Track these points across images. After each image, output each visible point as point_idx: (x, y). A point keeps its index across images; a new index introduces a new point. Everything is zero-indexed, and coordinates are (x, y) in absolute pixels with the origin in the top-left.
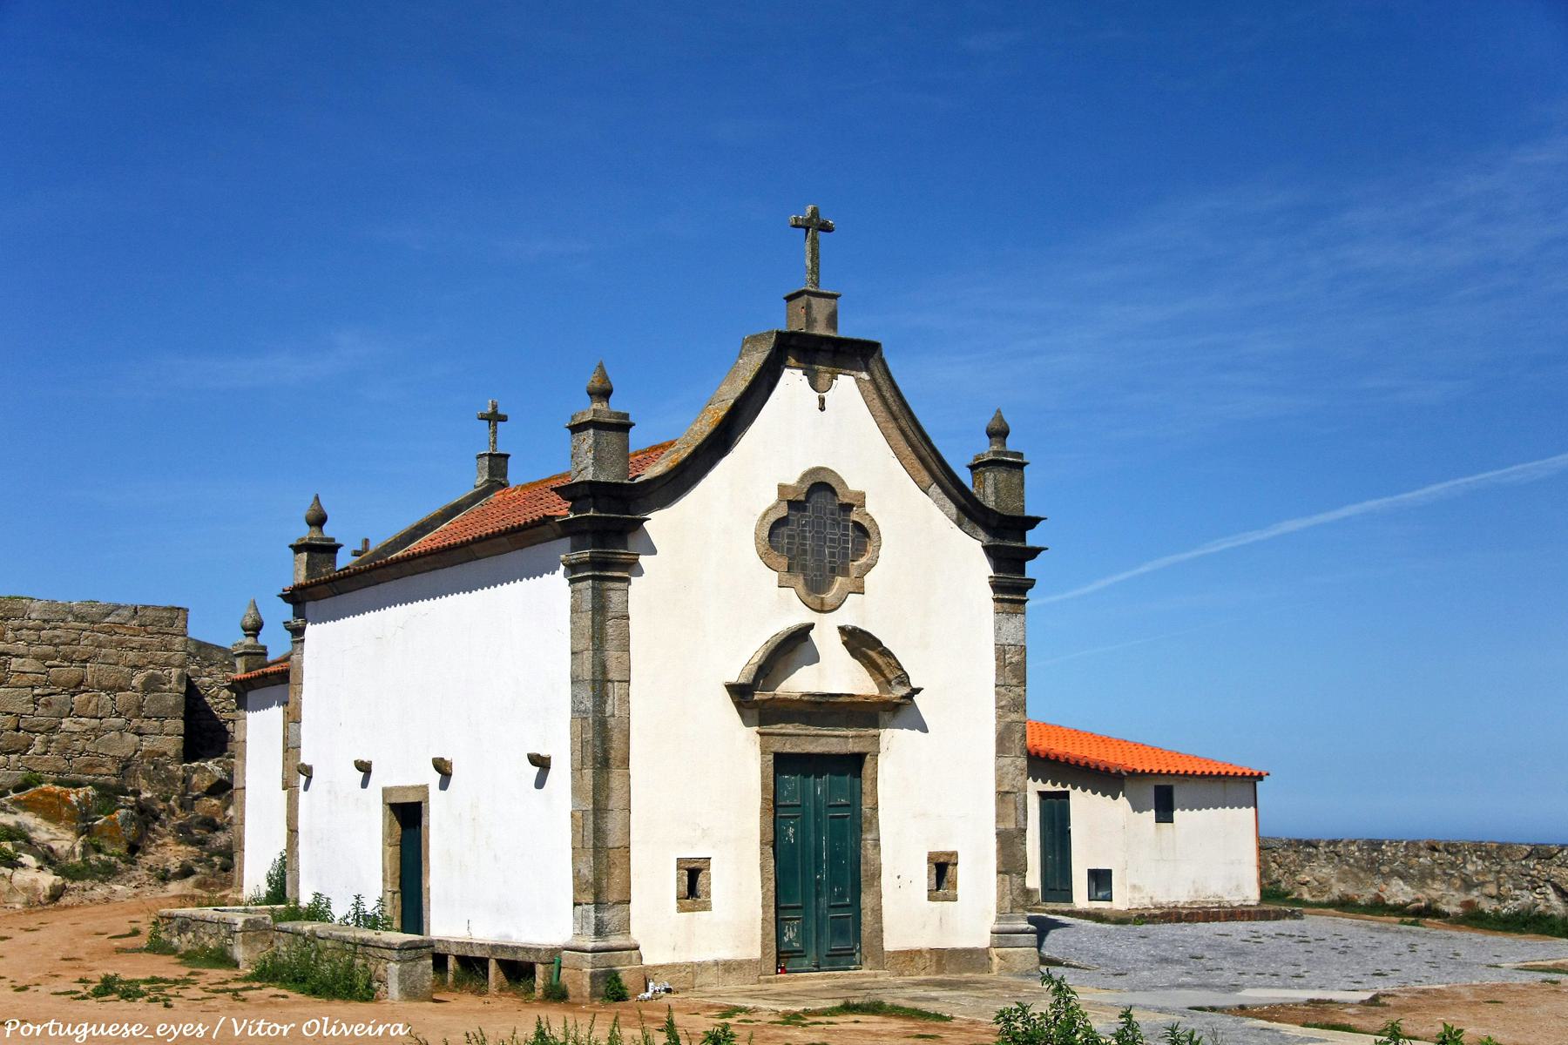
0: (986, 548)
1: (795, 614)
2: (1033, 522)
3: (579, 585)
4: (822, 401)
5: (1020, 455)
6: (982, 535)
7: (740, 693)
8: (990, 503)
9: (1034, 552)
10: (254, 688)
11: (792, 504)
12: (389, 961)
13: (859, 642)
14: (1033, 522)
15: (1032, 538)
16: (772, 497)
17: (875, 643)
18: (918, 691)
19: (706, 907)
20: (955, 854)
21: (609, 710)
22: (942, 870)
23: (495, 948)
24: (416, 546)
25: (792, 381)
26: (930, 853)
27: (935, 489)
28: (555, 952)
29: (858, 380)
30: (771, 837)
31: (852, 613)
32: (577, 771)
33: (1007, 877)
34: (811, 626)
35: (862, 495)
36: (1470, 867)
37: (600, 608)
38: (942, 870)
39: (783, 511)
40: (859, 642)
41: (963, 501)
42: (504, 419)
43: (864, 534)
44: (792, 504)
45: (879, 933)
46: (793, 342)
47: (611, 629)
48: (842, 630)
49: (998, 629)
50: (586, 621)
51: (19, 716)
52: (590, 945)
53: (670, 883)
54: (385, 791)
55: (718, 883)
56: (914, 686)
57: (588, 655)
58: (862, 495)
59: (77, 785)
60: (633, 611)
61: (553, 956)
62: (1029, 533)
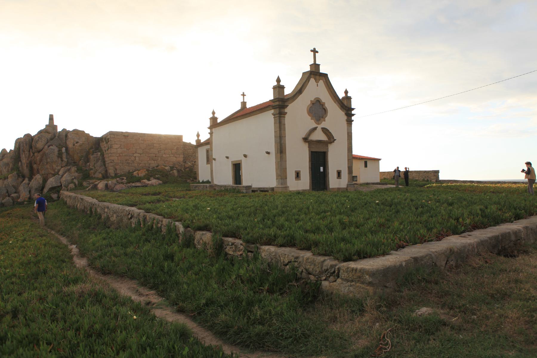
1: (315, 125)
2: (353, 109)
3: (276, 118)
4: (317, 85)
6: (345, 111)
7: (305, 139)
8: (346, 105)
9: (354, 115)
10: (200, 147)
11: (313, 104)
12: (243, 189)
14: (353, 109)
15: (353, 112)
16: (309, 103)
17: (328, 130)
18: (335, 140)
19: (300, 180)
20: (341, 171)
21: (282, 142)
22: (339, 174)
23: (259, 188)
24: (233, 117)
25: (312, 80)
27: (337, 102)
28: (274, 188)
29: (324, 81)
30: (311, 167)
31: (323, 125)
32: (276, 154)
34: (317, 127)
36: (414, 175)
37: (280, 123)
38: (339, 174)
39: (311, 105)
40: (325, 131)
42: (245, 95)
43: (325, 110)
44: (313, 104)
47: (282, 127)
48: (322, 128)
49: (348, 129)
50: (278, 125)
51: (156, 154)
52: (280, 186)
53: (294, 175)
54: (232, 162)
55: (302, 175)
57: (278, 132)
58: (325, 103)
59: (166, 166)
60: (286, 123)
61: (273, 189)
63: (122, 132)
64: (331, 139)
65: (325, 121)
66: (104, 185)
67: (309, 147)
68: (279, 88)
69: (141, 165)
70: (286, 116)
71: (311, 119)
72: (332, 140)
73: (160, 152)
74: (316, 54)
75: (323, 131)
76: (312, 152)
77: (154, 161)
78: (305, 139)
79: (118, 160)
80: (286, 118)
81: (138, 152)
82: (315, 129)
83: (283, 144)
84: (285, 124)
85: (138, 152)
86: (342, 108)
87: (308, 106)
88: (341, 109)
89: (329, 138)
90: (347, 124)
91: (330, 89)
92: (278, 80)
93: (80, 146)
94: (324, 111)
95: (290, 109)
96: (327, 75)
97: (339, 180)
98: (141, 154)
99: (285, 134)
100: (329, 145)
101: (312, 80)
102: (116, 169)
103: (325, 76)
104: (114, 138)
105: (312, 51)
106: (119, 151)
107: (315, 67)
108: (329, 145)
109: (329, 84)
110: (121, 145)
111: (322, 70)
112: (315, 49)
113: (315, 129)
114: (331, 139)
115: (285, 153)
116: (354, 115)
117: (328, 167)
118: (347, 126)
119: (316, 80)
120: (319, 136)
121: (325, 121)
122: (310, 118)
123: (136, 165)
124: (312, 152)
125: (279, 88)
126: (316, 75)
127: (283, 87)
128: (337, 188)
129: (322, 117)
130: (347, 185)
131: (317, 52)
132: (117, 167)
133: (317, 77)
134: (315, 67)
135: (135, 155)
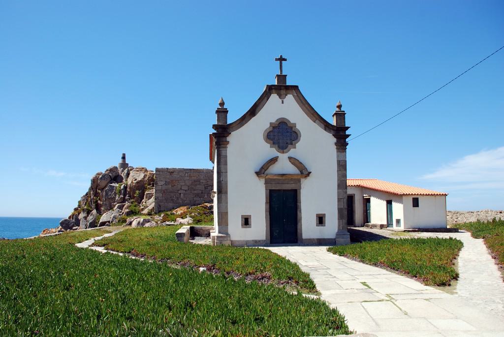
0: (333, 135)
5: (344, 111)
6: (332, 131)
9: (348, 136)
13: (293, 160)
15: (347, 132)
16: (268, 126)
18: (311, 172)
21: (222, 179)
25: (274, 97)
26: (317, 214)
27: (317, 121)
31: (292, 152)
33: (341, 220)
35: (295, 124)
38: (321, 220)
39: (271, 129)
40: (293, 160)
41: (325, 124)
45: (301, 234)
46: (273, 88)
47: (222, 160)
49: (338, 156)
56: (309, 171)
58: (295, 124)
60: (228, 155)
62: (346, 131)
63: (168, 169)
64: (305, 173)
65: (295, 148)
66: (137, 222)
67: (266, 183)
68: (222, 112)
69: (185, 202)
70: (228, 146)
71: (271, 147)
72: (305, 173)
73: (207, 188)
74: (283, 62)
75: (290, 161)
76: (271, 191)
77: (200, 198)
78: (258, 174)
79: (162, 197)
80: (228, 149)
81: (183, 188)
82: (274, 160)
83: (222, 182)
84: (226, 156)
85: (183, 188)
86: (327, 129)
87: (266, 130)
88: (325, 130)
89: (302, 173)
90: (337, 148)
91: (304, 105)
92: (222, 104)
93: (137, 183)
94: (294, 134)
95: (234, 138)
96: (298, 86)
97: (321, 228)
98: (186, 191)
99: (226, 169)
100: (303, 180)
101: (274, 97)
102: (160, 206)
103: (295, 88)
104: (159, 174)
105: (277, 60)
106: (164, 187)
107: (282, 78)
108: (303, 180)
109: (301, 98)
110: (166, 182)
111: (289, 83)
112: (281, 56)
113: (274, 160)
114: (305, 173)
115: (226, 193)
116: (348, 136)
117: (300, 211)
118: (337, 152)
119: (280, 96)
120: (284, 166)
121: (295, 148)
122: (269, 145)
123: (181, 202)
124: (271, 191)
125: (222, 112)
126: (281, 89)
127: (226, 112)
128: (318, 239)
129: (292, 144)
130: (337, 235)
131: (285, 60)
132: (161, 204)
133: (283, 92)
134: (282, 78)
135: (179, 192)
